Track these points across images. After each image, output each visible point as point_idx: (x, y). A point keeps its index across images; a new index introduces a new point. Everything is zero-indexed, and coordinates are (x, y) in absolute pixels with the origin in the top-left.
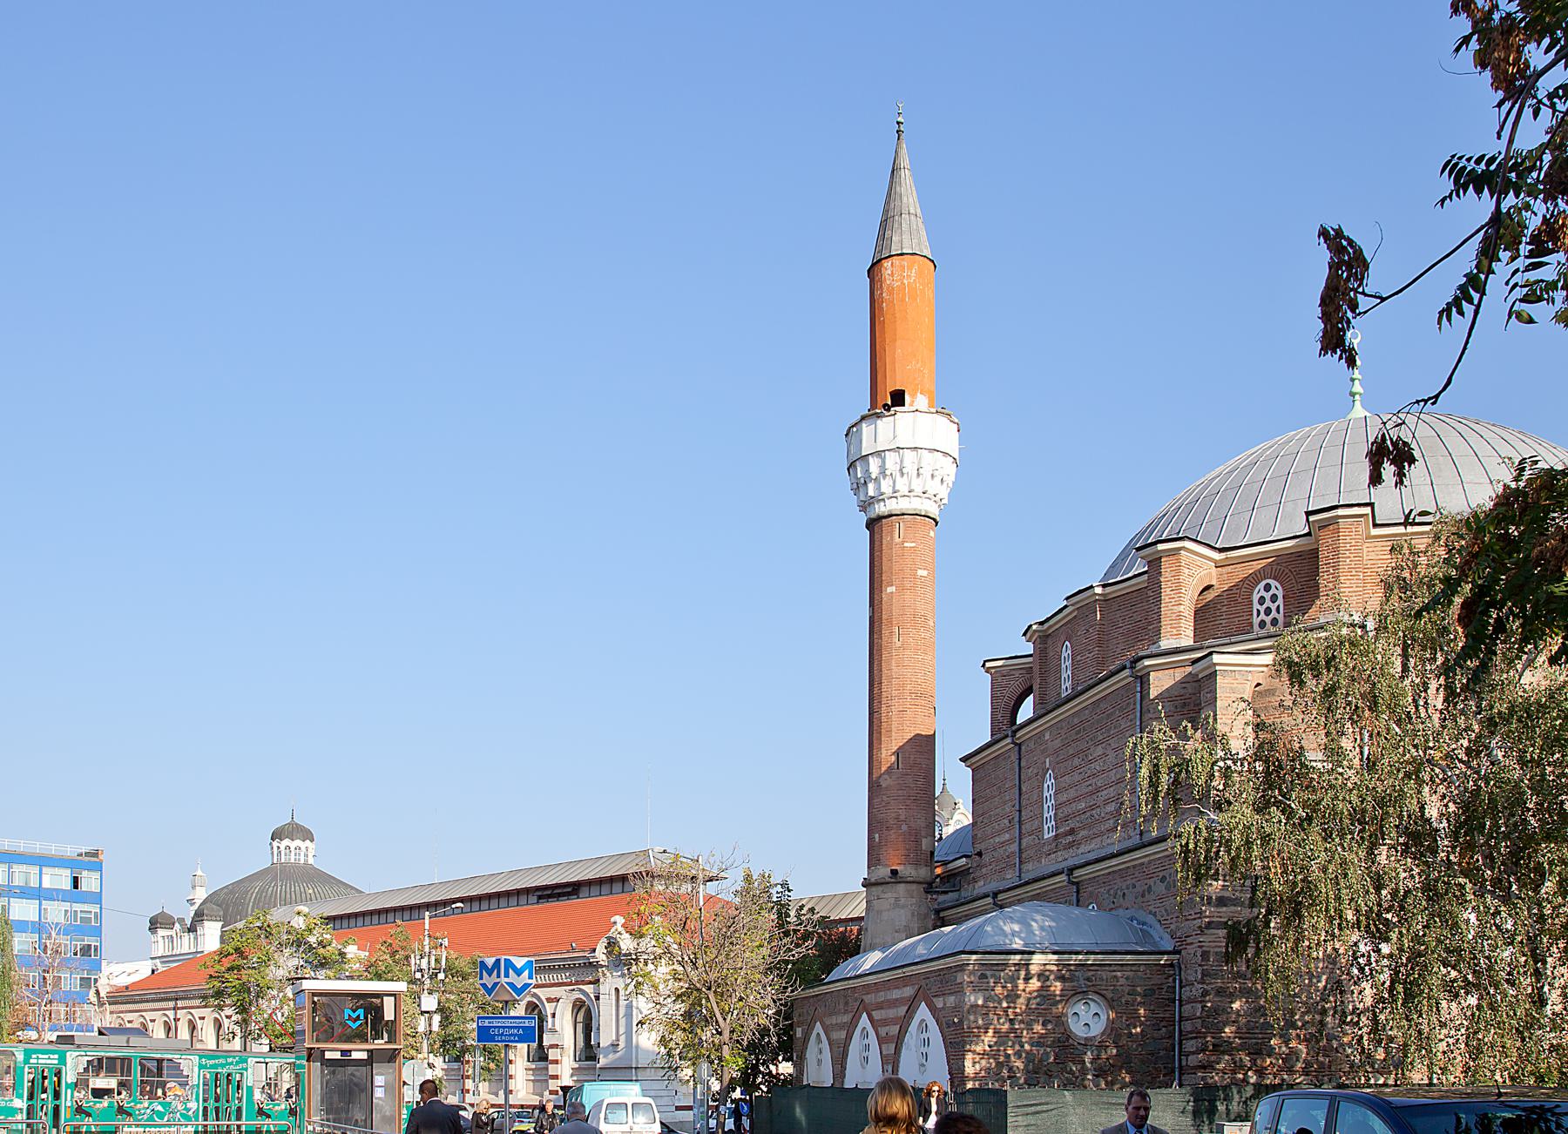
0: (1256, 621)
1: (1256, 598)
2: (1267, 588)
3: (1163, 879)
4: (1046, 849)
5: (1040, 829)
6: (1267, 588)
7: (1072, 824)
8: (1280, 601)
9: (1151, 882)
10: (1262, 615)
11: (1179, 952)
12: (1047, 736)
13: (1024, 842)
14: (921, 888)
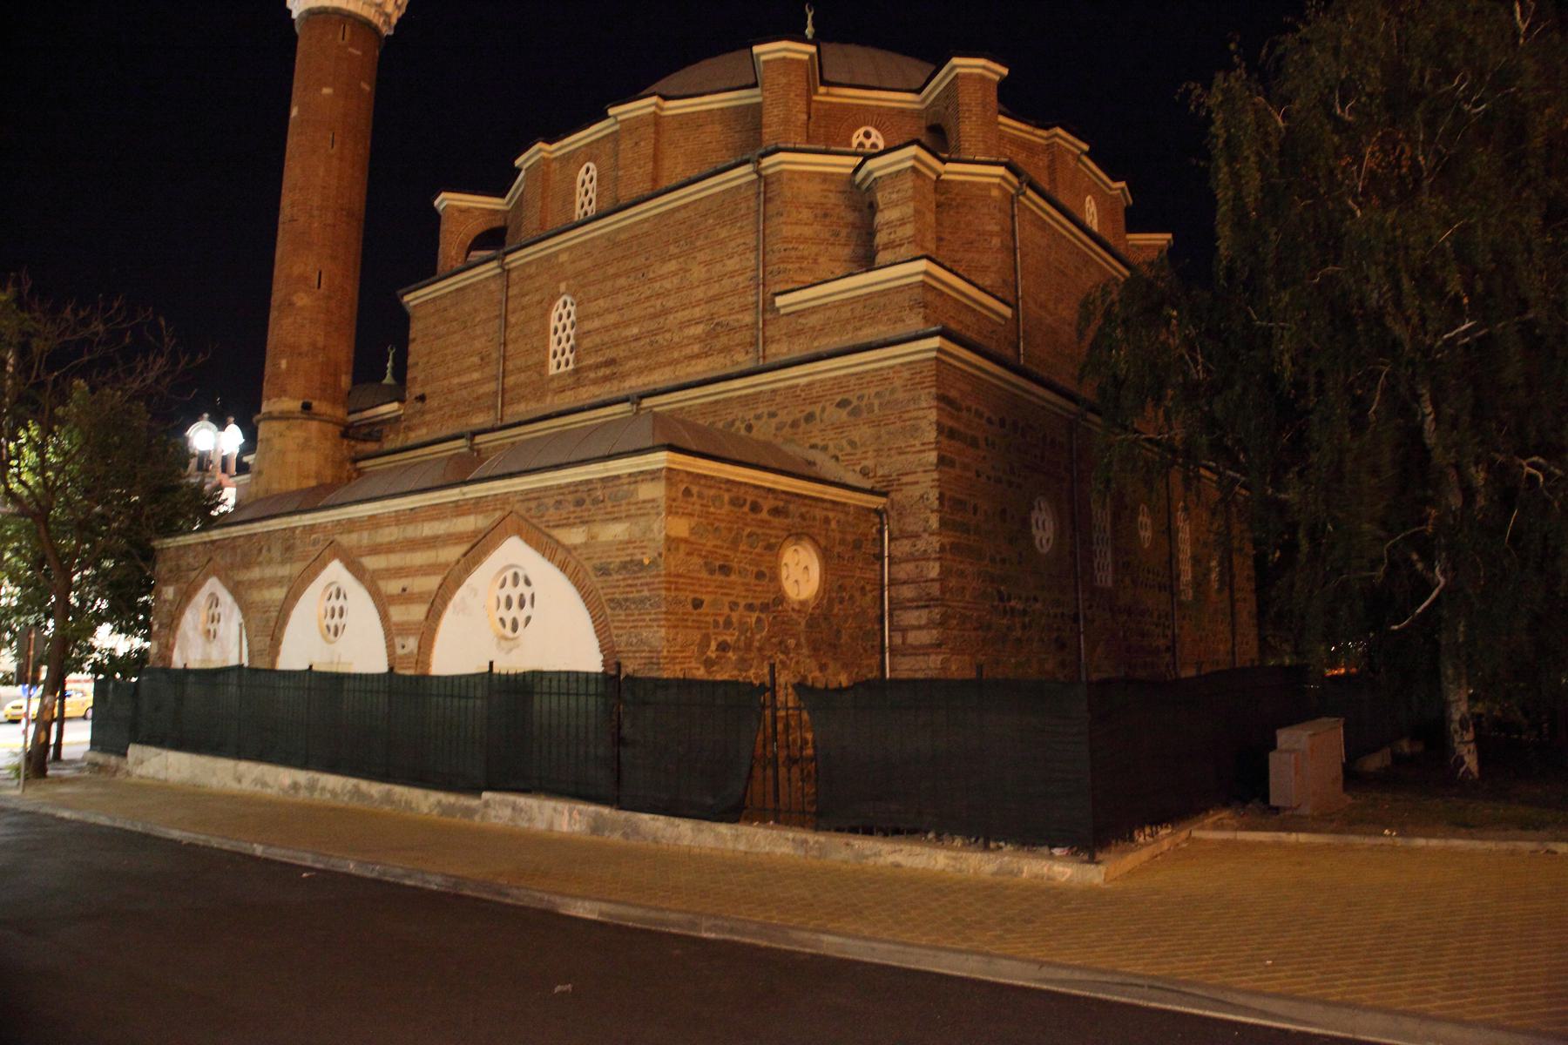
2: (867, 135)
3: (842, 404)
4: (555, 385)
5: (544, 364)
6: (867, 135)
9: (817, 409)
11: (885, 494)
12: (564, 258)
13: (510, 381)
14: (337, 430)
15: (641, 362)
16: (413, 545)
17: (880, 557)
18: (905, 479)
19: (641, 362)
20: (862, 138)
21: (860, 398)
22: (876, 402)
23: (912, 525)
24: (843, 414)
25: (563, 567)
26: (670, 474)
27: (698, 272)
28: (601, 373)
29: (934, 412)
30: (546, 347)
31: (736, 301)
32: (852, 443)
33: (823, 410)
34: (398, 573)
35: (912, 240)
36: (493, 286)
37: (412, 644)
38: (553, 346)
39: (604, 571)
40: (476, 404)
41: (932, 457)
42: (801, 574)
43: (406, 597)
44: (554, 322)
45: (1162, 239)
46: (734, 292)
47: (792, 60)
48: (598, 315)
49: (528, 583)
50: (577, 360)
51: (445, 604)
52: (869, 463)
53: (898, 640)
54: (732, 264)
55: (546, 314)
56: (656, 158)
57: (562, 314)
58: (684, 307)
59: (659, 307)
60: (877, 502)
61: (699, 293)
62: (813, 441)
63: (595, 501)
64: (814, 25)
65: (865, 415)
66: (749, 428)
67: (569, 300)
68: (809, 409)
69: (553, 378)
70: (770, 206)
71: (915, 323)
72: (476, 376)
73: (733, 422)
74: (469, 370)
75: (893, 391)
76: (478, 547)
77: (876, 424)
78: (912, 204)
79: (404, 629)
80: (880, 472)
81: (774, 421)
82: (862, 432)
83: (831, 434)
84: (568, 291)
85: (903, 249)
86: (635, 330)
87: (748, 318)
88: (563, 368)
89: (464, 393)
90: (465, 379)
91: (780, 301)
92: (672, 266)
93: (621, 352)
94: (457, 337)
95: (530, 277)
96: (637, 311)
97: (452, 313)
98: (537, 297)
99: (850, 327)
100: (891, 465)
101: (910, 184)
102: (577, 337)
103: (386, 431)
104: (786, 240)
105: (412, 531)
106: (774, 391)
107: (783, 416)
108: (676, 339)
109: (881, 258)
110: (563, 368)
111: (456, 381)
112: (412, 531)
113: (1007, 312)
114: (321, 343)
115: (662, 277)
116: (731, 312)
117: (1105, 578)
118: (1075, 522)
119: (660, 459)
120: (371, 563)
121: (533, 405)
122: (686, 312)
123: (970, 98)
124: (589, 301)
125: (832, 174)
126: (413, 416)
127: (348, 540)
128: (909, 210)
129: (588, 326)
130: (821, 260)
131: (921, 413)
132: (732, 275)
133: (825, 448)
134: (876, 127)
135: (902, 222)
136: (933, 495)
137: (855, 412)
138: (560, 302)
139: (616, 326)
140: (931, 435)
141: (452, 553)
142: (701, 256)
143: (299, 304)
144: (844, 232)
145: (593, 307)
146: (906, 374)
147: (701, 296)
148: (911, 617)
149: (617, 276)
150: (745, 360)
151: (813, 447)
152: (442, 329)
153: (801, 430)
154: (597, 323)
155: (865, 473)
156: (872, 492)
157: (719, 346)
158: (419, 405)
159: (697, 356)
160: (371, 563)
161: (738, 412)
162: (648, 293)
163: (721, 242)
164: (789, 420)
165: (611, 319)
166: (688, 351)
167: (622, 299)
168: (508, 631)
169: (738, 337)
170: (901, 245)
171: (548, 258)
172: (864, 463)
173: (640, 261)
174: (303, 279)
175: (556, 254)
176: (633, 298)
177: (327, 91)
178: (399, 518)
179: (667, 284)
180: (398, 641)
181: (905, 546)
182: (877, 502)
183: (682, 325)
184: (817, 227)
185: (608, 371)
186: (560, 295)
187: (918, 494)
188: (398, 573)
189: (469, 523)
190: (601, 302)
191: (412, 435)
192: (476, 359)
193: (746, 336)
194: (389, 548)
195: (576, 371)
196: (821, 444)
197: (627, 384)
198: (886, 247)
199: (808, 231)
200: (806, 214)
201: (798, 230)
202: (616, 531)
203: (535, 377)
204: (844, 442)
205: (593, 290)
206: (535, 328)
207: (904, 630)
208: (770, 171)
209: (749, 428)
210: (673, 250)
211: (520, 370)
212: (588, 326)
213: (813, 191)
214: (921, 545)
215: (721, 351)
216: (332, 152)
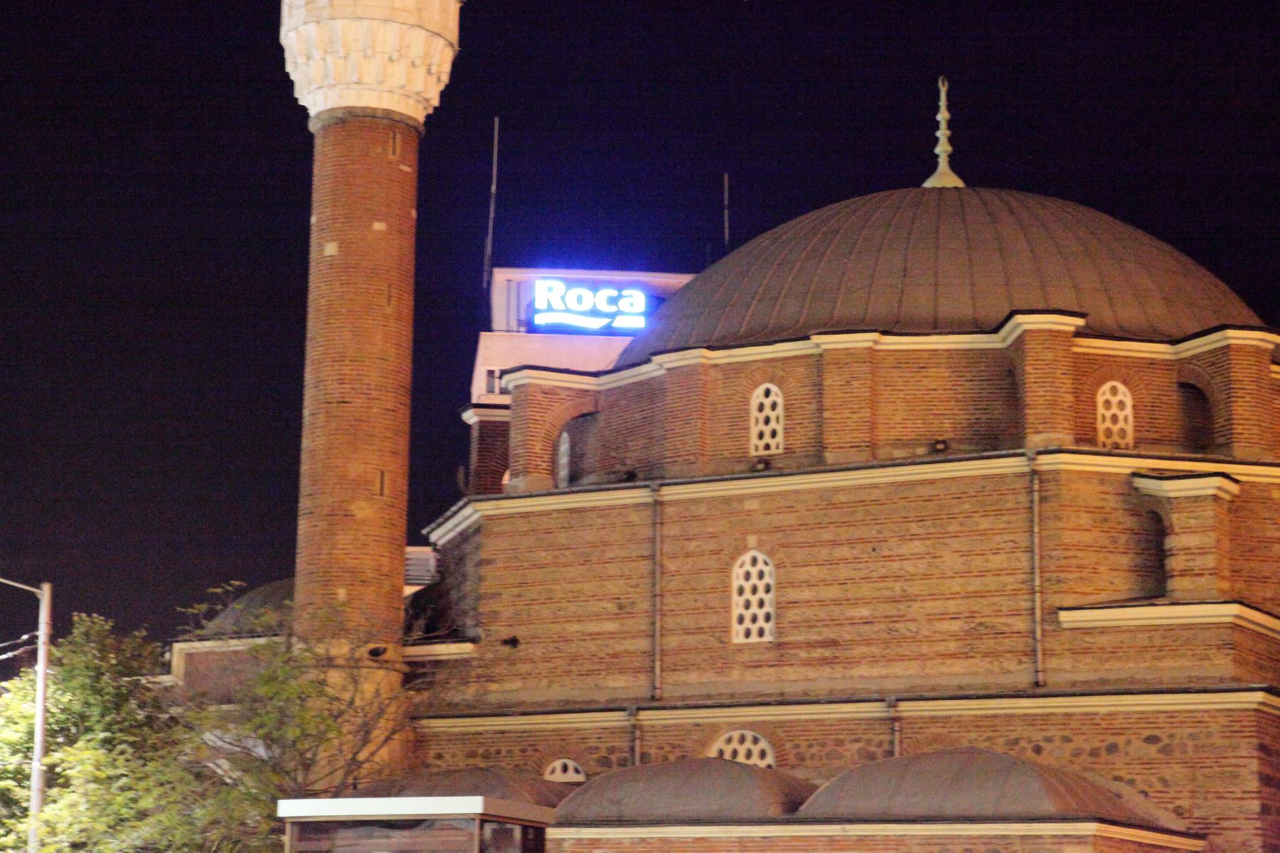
0: (1101, 427)
1: (1100, 399)
2: (1114, 391)
3: (1152, 740)
4: (746, 657)
5: (726, 630)
6: (1114, 391)
7: (830, 634)
8: (1129, 411)
9: (1121, 740)
10: (1108, 424)
15: (875, 650)
18: (1225, 824)
19: (875, 650)
20: (1108, 396)
21: (1172, 736)
22: (1190, 743)
24: (1152, 750)
27: (950, 561)
28: (818, 653)
29: (1255, 761)
30: (727, 609)
31: (1005, 604)
32: (1164, 781)
33: (1129, 742)
35: (1214, 572)
36: (634, 517)
38: (737, 610)
40: (615, 662)
41: (1255, 805)
44: (737, 580)
46: (1000, 592)
47: (1058, 332)
48: (809, 585)
50: (779, 631)
52: (1185, 803)
54: (998, 561)
55: (725, 570)
56: (873, 404)
57: (750, 572)
58: (933, 597)
59: (898, 591)
61: (955, 585)
62: (1117, 773)
64: (949, 108)
65: (1177, 754)
66: (1038, 750)
67: (761, 557)
68: (1111, 739)
69: (740, 649)
70: (1046, 506)
71: (1223, 665)
72: (610, 626)
73: (1016, 742)
74: (597, 617)
75: (1209, 735)
77: (1190, 765)
78: (1213, 534)
80: (1197, 814)
81: (1070, 747)
82: (1174, 772)
83: (1138, 769)
84: (760, 546)
85: (1203, 580)
86: (865, 612)
87: (1020, 624)
88: (754, 638)
89: (592, 647)
90: (592, 627)
91: (1064, 616)
92: (917, 547)
93: (846, 633)
94: (573, 572)
96: (865, 590)
97: (562, 538)
98: (712, 545)
99: (1148, 656)
100: (1208, 809)
101: (1210, 513)
102: (779, 606)
106: (1068, 715)
107: (1079, 742)
108: (925, 632)
109: (1175, 584)
110: (754, 638)
111: (574, 628)
114: (385, 570)
115: (902, 558)
119: (1090, 828)
121: (709, 676)
122: (939, 603)
123: (1242, 372)
124: (795, 565)
125: (1110, 474)
128: (1209, 539)
130: (1102, 569)
131: (1239, 761)
132: (998, 573)
133: (1131, 782)
134: (1125, 383)
135: (1203, 551)
137: (1166, 750)
138: (747, 557)
139: (836, 602)
140: (1254, 784)
142: (955, 544)
143: (360, 515)
144: (1123, 539)
145: (802, 574)
146: (1223, 721)
147: (957, 589)
149: (835, 543)
150: (1021, 675)
151: (1117, 779)
153: (1102, 760)
154: (807, 594)
155: (1179, 812)
157: (983, 648)
158: (507, 649)
159: (953, 656)
161: (1020, 730)
162: (883, 572)
163: (983, 533)
166: (940, 648)
167: (844, 572)
169: (1007, 643)
170: (1202, 575)
171: (727, 500)
172: (1178, 803)
173: (870, 532)
174: (361, 483)
175: (740, 499)
176: (861, 574)
177: (379, 226)
179: (909, 567)
183: (932, 618)
184: (1096, 533)
185: (827, 653)
186: (746, 549)
187: (1239, 840)
190: (814, 570)
191: (493, 687)
192: (611, 607)
193: (1020, 643)
195: (779, 646)
196: (1128, 777)
198: (1184, 573)
199: (1087, 538)
200: (1085, 519)
201: (1077, 537)
204: (1154, 780)
205: (800, 555)
206: (709, 583)
208: (1045, 468)
210: (914, 528)
211: (687, 631)
212: (793, 594)
213: (1091, 494)
215: (986, 655)
216: (389, 310)
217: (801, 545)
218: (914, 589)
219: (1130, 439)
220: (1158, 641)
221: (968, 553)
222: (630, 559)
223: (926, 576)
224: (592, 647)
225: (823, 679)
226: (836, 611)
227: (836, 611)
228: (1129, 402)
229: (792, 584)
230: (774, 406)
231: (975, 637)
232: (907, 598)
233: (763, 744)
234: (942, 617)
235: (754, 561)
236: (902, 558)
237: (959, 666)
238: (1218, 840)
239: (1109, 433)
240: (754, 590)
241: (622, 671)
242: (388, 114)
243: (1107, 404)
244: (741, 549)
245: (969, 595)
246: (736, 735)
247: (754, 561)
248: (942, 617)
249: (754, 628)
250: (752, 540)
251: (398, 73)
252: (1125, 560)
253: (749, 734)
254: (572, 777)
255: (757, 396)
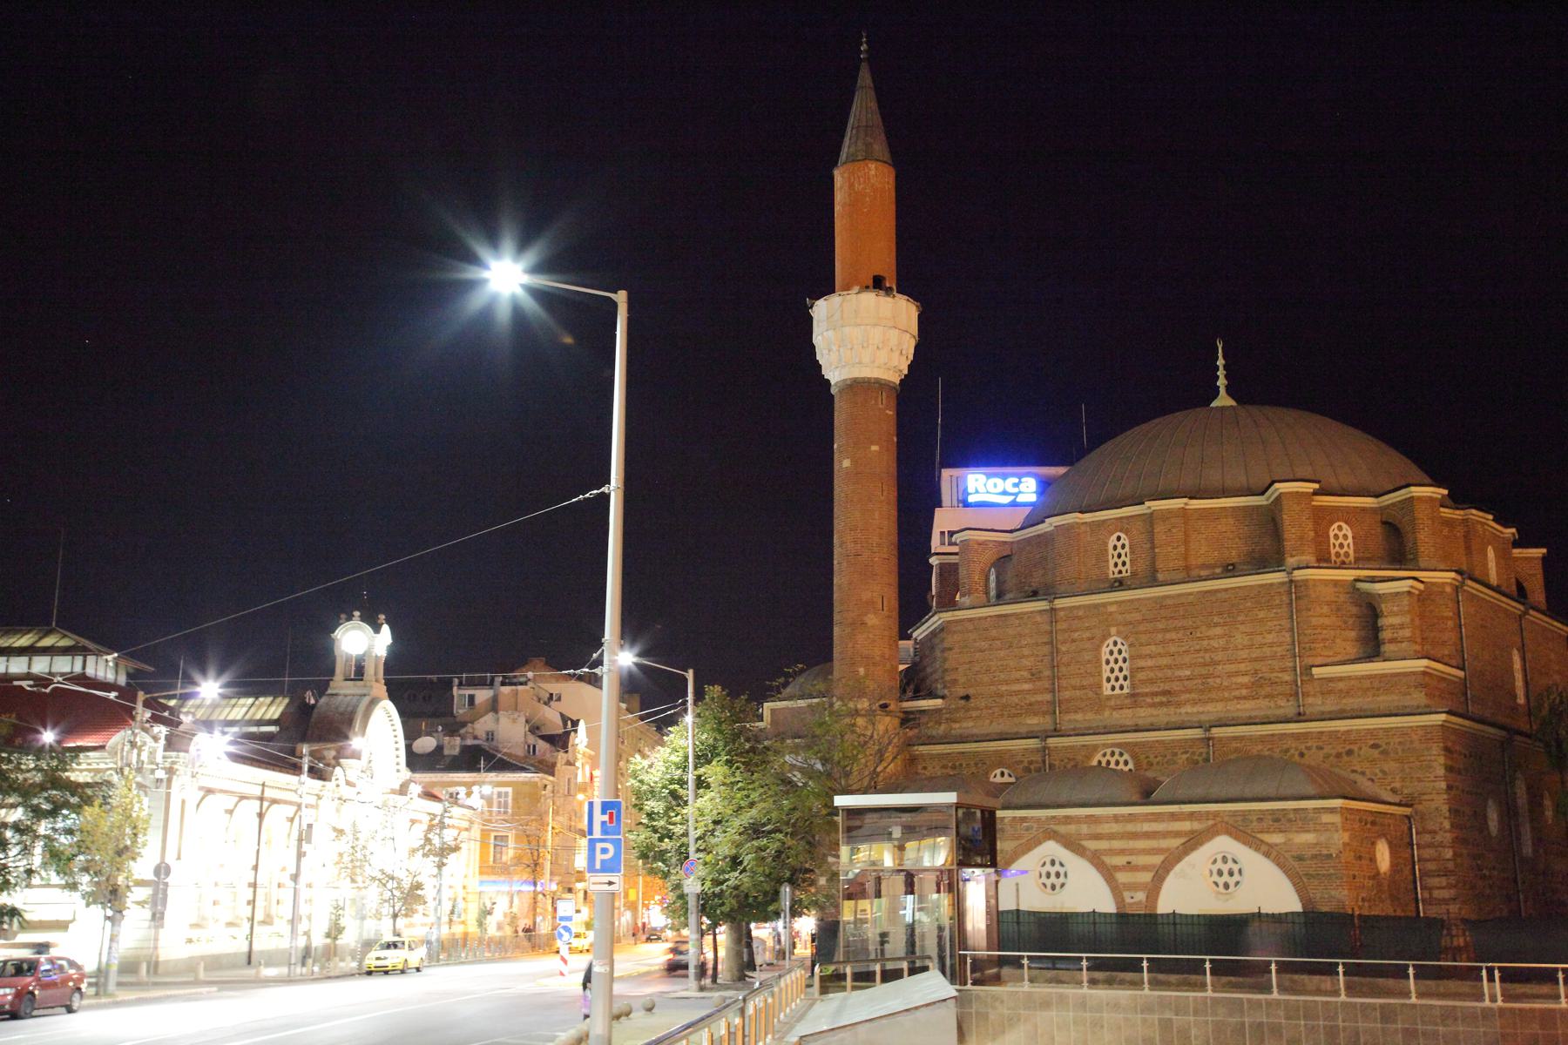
0: (1333, 552)
1: (1332, 534)
2: (1340, 528)
3: (1375, 746)
5: (1100, 687)
6: (1340, 528)
8: (1350, 540)
16: (1135, 836)
17: (1412, 845)
23: (1431, 826)
24: (1376, 753)
25: (1267, 855)
26: (1343, 810)
27: (1240, 639)
28: (1157, 699)
30: (1100, 674)
34: (1122, 852)
35: (1411, 640)
36: (1039, 619)
37: (1140, 896)
39: (1300, 858)
41: (1443, 785)
42: (1383, 857)
43: (1129, 867)
44: (1105, 655)
45: (1539, 552)
46: (1273, 657)
49: (1235, 862)
50: (1133, 686)
51: (1168, 872)
52: (1397, 785)
53: (1427, 895)
54: (1270, 638)
55: (1098, 648)
56: (1186, 542)
57: (1113, 652)
58: (1230, 662)
60: (1407, 811)
61: (1244, 654)
63: (1290, 821)
66: (1302, 755)
67: (1119, 641)
69: (1109, 698)
70: (1301, 602)
72: (1026, 686)
73: (1287, 751)
74: (1017, 681)
76: (1194, 841)
79: (1133, 887)
81: (1321, 753)
82: (1391, 766)
84: (1119, 633)
86: (1188, 673)
87: (1287, 677)
88: (1117, 691)
89: (1015, 699)
90: (1016, 687)
91: (1315, 670)
92: (1218, 631)
93: (1176, 686)
94: (1002, 653)
95: (1080, 618)
96: (1187, 659)
97: (994, 633)
98: (1088, 634)
101: (1406, 602)
102: (1132, 671)
103: (924, 719)
104: (1315, 628)
105: (1130, 827)
107: (1327, 750)
109: (1387, 648)
110: (1117, 691)
111: (1004, 688)
112: (1130, 827)
113: (1461, 674)
115: (1209, 638)
116: (1272, 670)
117: (1528, 850)
118: (1509, 812)
120: (1092, 845)
121: (1090, 716)
123: (1422, 513)
126: (957, 710)
127: (1062, 829)
128: (1406, 619)
129: (1141, 663)
132: (1271, 645)
133: (1363, 773)
135: (1402, 626)
136: (1445, 808)
137: (1385, 753)
139: (1169, 667)
140: (1441, 772)
141: (1175, 843)
142: (1242, 628)
143: (870, 623)
144: (1351, 621)
145: (1146, 650)
148: (1435, 881)
149: (1165, 630)
150: (1289, 708)
152: (984, 645)
154: (1150, 663)
155: (1394, 791)
156: (1399, 805)
158: (963, 702)
159: (1245, 698)
160: (1092, 845)
161: (1290, 743)
164: (1334, 752)
165: (1165, 661)
166: (1237, 693)
168: (1221, 888)
171: (1096, 606)
174: (871, 602)
175: (1104, 605)
177: (874, 448)
178: (1116, 818)
180: (1127, 895)
181: (1427, 838)
182: (1407, 811)
186: (1110, 635)
188: (1122, 852)
189: (1186, 826)
190: (1153, 648)
192: (1025, 674)
194: (1111, 837)
195: (1132, 695)
197: (1183, 710)
198: (1392, 641)
199: (1327, 621)
200: (1325, 609)
201: (1322, 620)
202: (1310, 838)
203: (1091, 694)
205: (1144, 638)
207: (1430, 889)
209: (1302, 755)
210: (1216, 619)
211: (1074, 688)
212: (1141, 663)
213: (1328, 593)
214: (1438, 838)
217: (1145, 632)
218: (1219, 656)
219: (1352, 558)
220: (1376, 684)
221: (1252, 634)
222: (1037, 644)
223: (1225, 649)
224: (1015, 699)
225: (1162, 715)
226: (1169, 673)
227: (1169, 673)
228: (1350, 535)
229: (1140, 657)
230: (1123, 546)
231: (1258, 686)
232: (1215, 663)
233: (1126, 756)
234: (1237, 673)
235: (1115, 643)
236: (1209, 638)
237: (1248, 705)
238: (1420, 807)
239: (1338, 555)
240: (1116, 661)
241: (1035, 714)
242: (878, 381)
243: (1336, 537)
244: (1105, 637)
245: (1256, 660)
246: (1109, 751)
247: (1115, 643)
248: (1237, 673)
249: (1117, 685)
250: (1113, 630)
251: (882, 356)
252: (1353, 634)
253: (1117, 751)
254: (1006, 779)
255: (1112, 540)
